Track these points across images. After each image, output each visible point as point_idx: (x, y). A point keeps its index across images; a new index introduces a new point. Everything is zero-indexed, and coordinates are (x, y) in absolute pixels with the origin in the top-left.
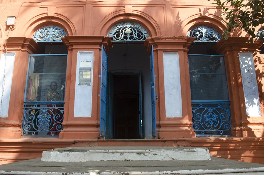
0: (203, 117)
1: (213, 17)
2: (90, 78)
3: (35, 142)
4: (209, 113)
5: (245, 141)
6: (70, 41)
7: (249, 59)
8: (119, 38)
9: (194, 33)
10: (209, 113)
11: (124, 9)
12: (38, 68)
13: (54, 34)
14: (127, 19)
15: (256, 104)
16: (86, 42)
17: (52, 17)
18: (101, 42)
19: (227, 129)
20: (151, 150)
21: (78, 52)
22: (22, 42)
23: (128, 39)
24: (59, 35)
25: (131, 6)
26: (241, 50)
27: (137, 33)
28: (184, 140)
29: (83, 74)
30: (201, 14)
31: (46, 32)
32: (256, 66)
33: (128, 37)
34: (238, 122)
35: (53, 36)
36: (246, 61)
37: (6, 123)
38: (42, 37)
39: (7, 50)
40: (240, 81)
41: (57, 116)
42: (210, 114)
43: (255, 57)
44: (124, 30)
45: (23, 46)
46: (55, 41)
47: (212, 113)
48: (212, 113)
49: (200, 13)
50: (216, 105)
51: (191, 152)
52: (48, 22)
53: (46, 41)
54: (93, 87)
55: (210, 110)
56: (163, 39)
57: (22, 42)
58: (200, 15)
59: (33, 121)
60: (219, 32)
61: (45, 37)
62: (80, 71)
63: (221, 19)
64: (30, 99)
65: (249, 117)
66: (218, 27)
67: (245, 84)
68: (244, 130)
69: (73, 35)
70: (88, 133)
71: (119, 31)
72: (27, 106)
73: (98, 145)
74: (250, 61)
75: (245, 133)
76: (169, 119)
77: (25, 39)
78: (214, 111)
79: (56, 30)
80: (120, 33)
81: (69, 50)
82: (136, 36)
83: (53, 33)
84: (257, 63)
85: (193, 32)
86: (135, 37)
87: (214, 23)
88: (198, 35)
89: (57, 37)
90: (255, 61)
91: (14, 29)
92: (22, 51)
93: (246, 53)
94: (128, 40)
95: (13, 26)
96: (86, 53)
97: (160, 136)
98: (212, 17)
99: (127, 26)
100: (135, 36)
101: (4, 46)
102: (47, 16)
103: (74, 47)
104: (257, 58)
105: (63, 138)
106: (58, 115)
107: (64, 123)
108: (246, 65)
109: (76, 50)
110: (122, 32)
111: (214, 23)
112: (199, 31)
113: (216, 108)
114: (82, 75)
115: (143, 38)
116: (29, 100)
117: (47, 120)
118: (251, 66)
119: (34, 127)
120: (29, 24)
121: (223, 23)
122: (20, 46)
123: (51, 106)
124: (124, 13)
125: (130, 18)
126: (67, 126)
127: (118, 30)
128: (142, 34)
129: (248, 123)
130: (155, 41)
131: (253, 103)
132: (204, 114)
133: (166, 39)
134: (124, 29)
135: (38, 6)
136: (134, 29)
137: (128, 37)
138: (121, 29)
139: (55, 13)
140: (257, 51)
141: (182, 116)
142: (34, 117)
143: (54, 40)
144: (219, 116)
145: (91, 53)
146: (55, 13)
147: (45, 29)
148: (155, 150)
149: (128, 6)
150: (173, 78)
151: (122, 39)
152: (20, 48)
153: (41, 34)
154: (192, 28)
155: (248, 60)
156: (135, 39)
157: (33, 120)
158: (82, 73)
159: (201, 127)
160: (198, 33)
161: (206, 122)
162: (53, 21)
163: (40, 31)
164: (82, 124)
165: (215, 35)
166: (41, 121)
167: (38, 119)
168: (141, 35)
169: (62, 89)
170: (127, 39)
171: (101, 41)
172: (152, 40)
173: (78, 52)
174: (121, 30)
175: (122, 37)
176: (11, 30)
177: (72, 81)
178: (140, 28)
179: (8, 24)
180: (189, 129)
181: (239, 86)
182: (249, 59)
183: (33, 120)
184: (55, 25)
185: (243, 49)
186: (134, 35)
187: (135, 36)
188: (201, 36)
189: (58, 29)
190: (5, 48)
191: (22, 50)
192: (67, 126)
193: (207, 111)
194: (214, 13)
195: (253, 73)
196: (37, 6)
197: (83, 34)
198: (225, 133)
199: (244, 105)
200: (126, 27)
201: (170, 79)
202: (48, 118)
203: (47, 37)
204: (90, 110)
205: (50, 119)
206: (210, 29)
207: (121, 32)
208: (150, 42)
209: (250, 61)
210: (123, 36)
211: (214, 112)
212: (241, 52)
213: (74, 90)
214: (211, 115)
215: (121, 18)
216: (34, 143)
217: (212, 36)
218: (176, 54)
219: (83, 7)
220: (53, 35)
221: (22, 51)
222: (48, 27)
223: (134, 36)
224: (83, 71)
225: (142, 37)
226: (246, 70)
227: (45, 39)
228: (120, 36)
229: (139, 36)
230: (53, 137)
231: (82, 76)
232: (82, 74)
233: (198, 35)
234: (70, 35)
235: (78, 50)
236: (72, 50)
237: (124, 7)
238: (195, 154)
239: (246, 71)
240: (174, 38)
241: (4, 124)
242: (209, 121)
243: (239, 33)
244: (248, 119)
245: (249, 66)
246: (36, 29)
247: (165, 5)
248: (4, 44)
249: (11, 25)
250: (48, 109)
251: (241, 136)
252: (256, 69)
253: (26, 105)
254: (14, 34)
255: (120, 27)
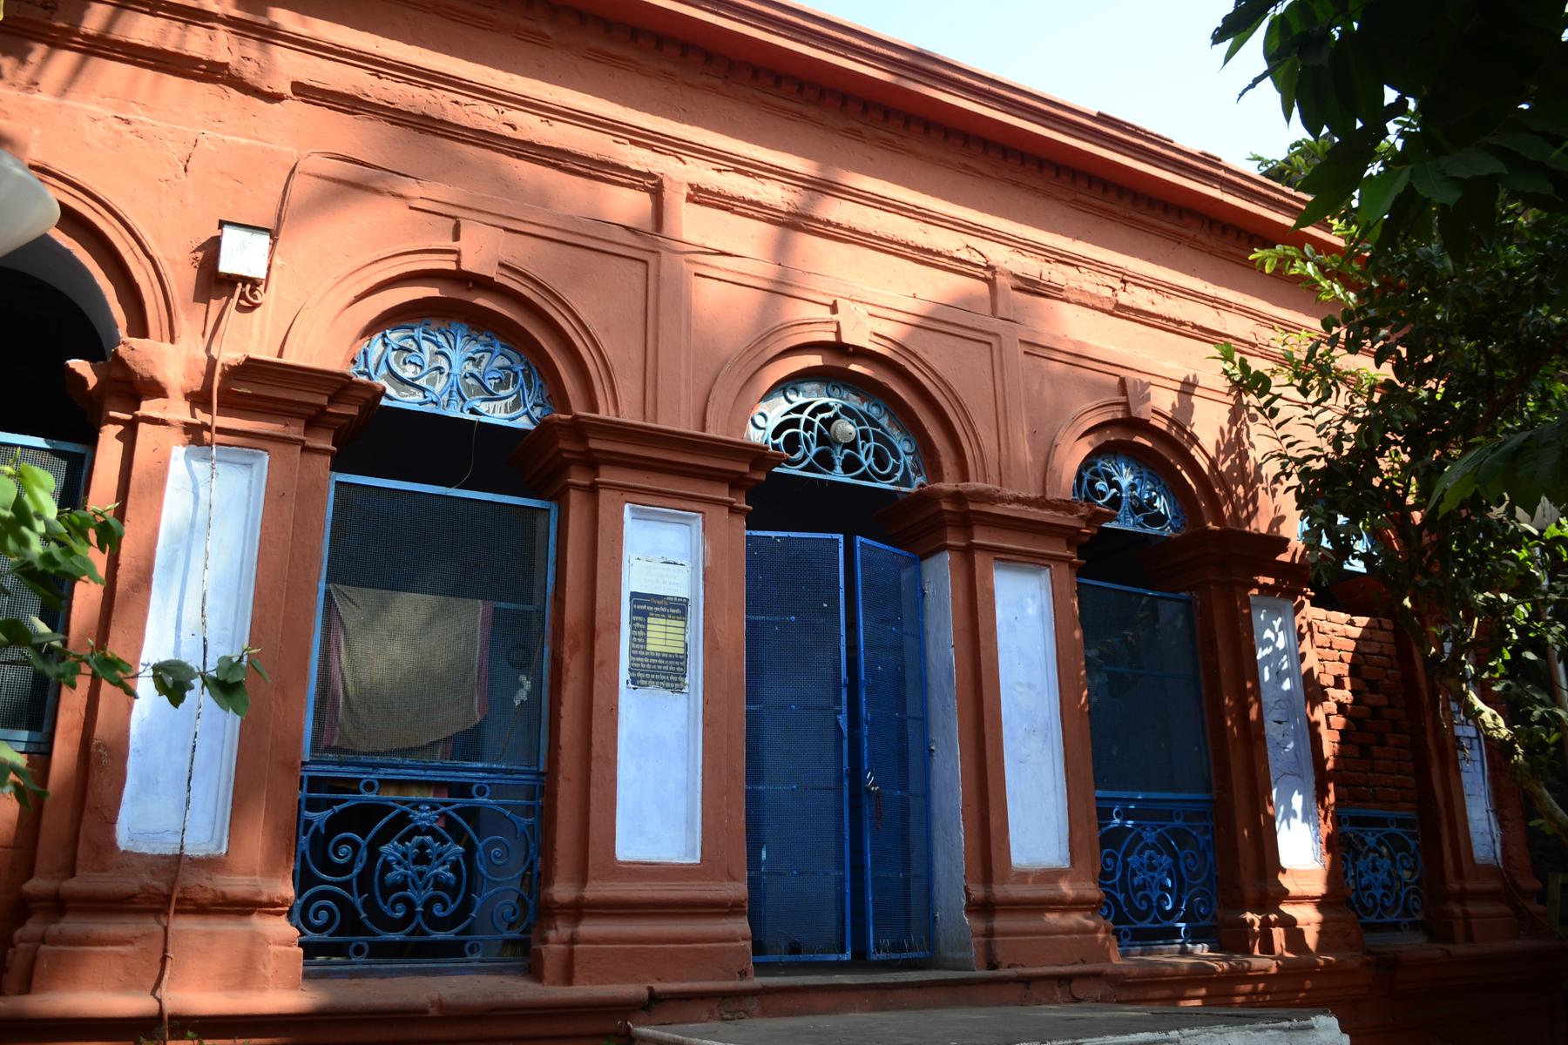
0: (1126, 864)
1: (1164, 428)
2: (682, 651)
3: (440, 1005)
4: (1147, 846)
5: (1287, 970)
6: (593, 444)
7: (1277, 623)
8: (798, 456)
9: (1091, 484)
10: (1147, 846)
11: (835, 317)
12: (368, 553)
13: (472, 375)
14: (838, 364)
15: (1300, 815)
16: (684, 465)
17: (481, 283)
18: (742, 474)
19: (1204, 917)
20: (1186, 1031)
21: (627, 506)
22: (324, 400)
23: (839, 469)
24: (503, 384)
25: (862, 310)
26: (1256, 585)
27: (872, 444)
28: (1097, 976)
29: (649, 627)
30: (1126, 404)
31: (427, 357)
32: (1303, 657)
33: (838, 458)
34: (1250, 891)
35: (468, 387)
36: (1268, 634)
37: (223, 894)
38: (403, 381)
39: (220, 430)
40: (1253, 715)
41: (495, 851)
42: (1147, 853)
43: (1298, 618)
44: (817, 421)
45: (315, 420)
46: (483, 419)
47: (1153, 847)
48: (1153, 847)
49: (1123, 399)
50: (1169, 816)
51: (1299, 1033)
52: (452, 303)
53: (429, 408)
54: (706, 702)
55: (1149, 836)
56: (1002, 500)
57: (324, 400)
58: (1121, 408)
59: (359, 876)
60: (1175, 488)
61: (421, 382)
62: (634, 612)
63: (1194, 439)
64: (335, 743)
65: (1284, 871)
66: (1179, 472)
67: (1271, 730)
68: (1277, 924)
69: (596, 410)
70: (695, 949)
71: (794, 423)
72: (315, 783)
73: (765, 1013)
74: (1281, 634)
75: (1278, 934)
76: (1023, 876)
77: (338, 385)
78: (1160, 837)
79: (487, 355)
80: (801, 431)
81: (577, 487)
82: (871, 459)
83: (470, 367)
84: (1306, 646)
85: (1087, 476)
86: (866, 464)
87: (1163, 451)
88: (1103, 494)
89: (492, 397)
90: (1301, 637)
91: (258, 305)
92: (306, 449)
93: (1268, 600)
94: (838, 476)
95: (254, 283)
96: (663, 519)
97: (1000, 954)
98: (1162, 425)
99: (831, 401)
100: (867, 462)
101: (199, 399)
102: (453, 267)
103: (606, 475)
104: (1304, 623)
105: (568, 979)
106: (497, 843)
107: (562, 891)
108: (1268, 651)
109: (615, 495)
110: (809, 426)
111: (1163, 451)
112: (1109, 476)
113: (1170, 825)
114: (641, 633)
115: (899, 475)
116: (329, 749)
117: (440, 869)
118: (1285, 651)
119: (364, 915)
120: (351, 297)
121: (1198, 458)
122: (299, 416)
123: (463, 790)
124: (831, 338)
125: (854, 367)
126: (579, 910)
127: (794, 416)
128: (897, 456)
129: (1284, 895)
130: (972, 507)
131: (1290, 813)
132: (1127, 854)
133: (1010, 502)
134: (820, 416)
135: (401, 196)
136: (860, 423)
137: (838, 458)
138: (804, 416)
139: (502, 265)
140: (1304, 594)
141: (1067, 865)
142: (364, 854)
143: (473, 411)
144: (1176, 864)
145: (686, 521)
146: (502, 265)
147: (418, 333)
148: (1195, 1031)
149: (853, 306)
150: (1030, 686)
151: (810, 464)
152: (295, 430)
153: (397, 359)
154: (1088, 462)
155: (1273, 629)
156: (864, 476)
157: (356, 871)
158: (646, 623)
159: (1131, 916)
160: (1101, 485)
161: (1136, 890)
162: (482, 301)
163: (394, 337)
164: (660, 900)
165: (1161, 504)
166: (406, 876)
167: (387, 867)
168: (892, 460)
169: (522, 695)
170: (831, 467)
171: (745, 468)
172: (958, 497)
173: (627, 506)
174: (804, 416)
175: (811, 455)
176: (240, 308)
177: (602, 663)
178: (884, 421)
179: (226, 266)
180: (1091, 923)
181: (1254, 735)
182: (1277, 623)
183: (356, 871)
184: (481, 324)
185: (1262, 580)
186: (863, 453)
187: (867, 462)
188: (1115, 502)
189: (497, 350)
190: (194, 416)
191: (311, 442)
192: (579, 910)
193: (1139, 837)
194: (1166, 408)
195: (1293, 683)
196: (394, 195)
197: (649, 412)
198: (1196, 936)
199: (1272, 820)
200: (825, 408)
201: (1020, 689)
202: (444, 863)
203: (432, 382)
204: (690, 822)
205: (455, 868)
206: (1145, 475)
207: (806, 430)
208: (945, 506)
209: (1281, 634)
210: (814, 449)
211: (1162, 845)
212: (1255, 591)
213: (613, 711)
214: (1151, 858)
215: (815, 360)
216: (433, 1012)
217: (1152, 501)
218: (1037, 572)
219: (645, 262)
220: (470, 381)
221: (306, 449)
222: (435, 324)
223: (862, 457)
224: (646, 614)
225: (896, 468)
226: (1266, 669)
227: (419, 397)
228: (803, 447)
229: (881, 461)
230: (478, 971)
231: (645, 638)
232: (645, 630)
233: (1103, 494)
234: (579, 410)
235: (627, 496)
236: (593, 490)
237: (834, 308)
238: (1310, 1039)
239: (1267, 677)
240: (1042, 503)
241: (209, 896)
242: (1143, 886)
243: (1251, 507)
244: (1281, 878)
245: (1277, 654)
246: (370, 330)
247: (997, 335)
248: (197, 384)
249: (245, 280)
250: (442, 809)
251: (1268, 948)
252: (1305, 667)
253: (310, 778)
254: (246, 338)
255: (799, 400)
